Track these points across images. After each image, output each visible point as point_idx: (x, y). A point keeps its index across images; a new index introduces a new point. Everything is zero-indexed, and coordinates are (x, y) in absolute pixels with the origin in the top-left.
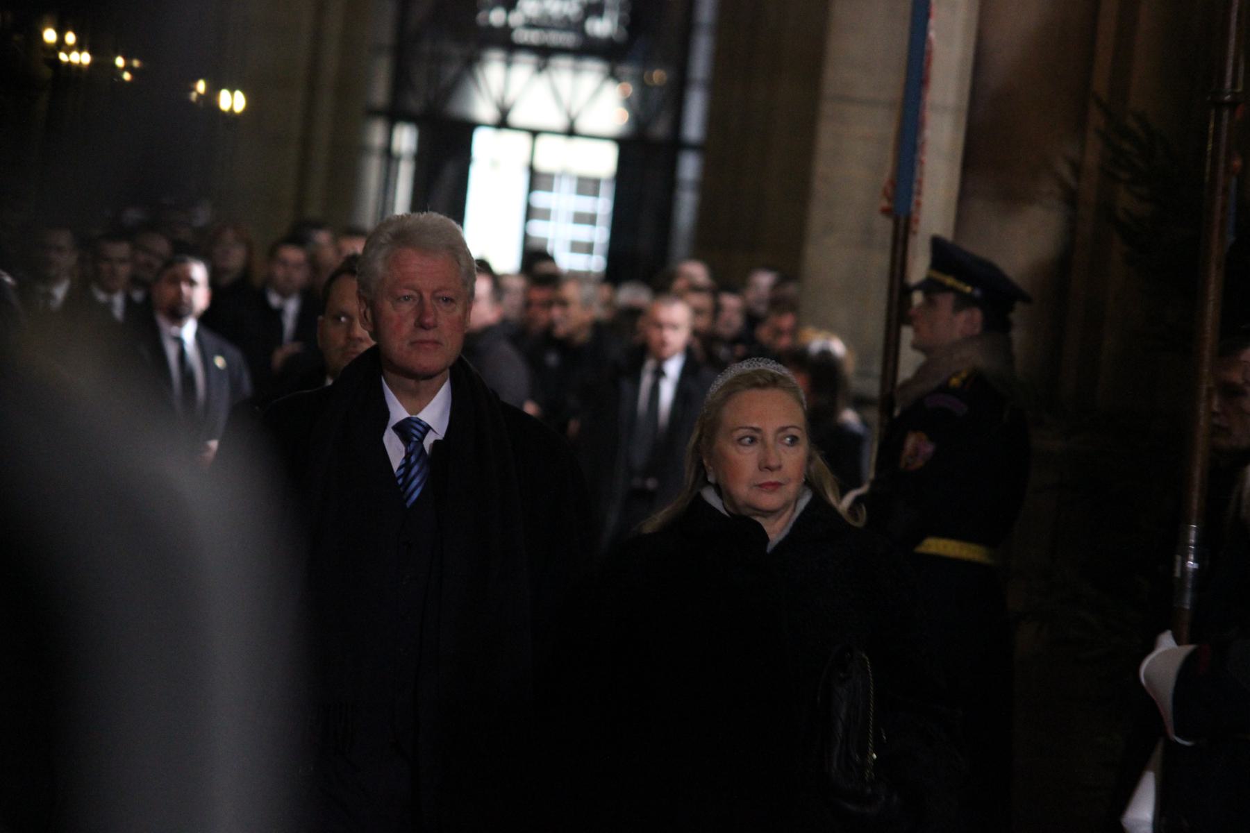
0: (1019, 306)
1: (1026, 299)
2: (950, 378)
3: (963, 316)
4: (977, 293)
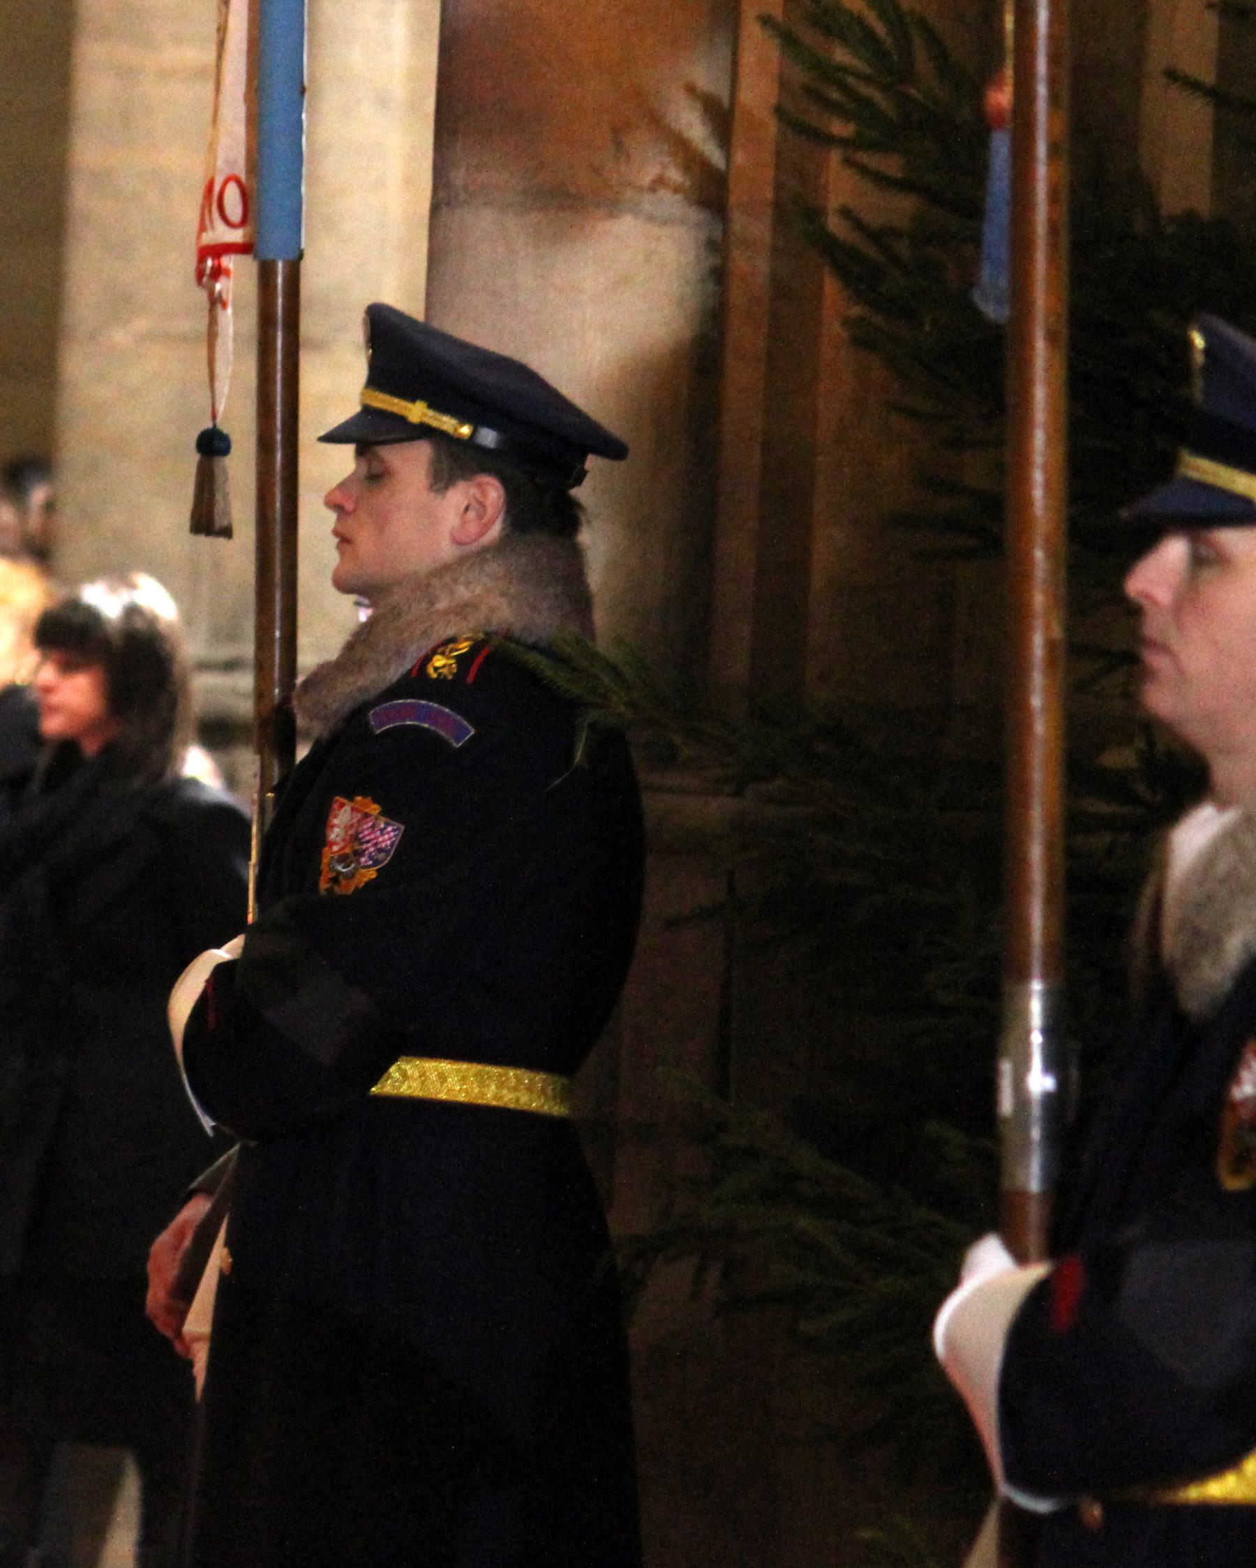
0: (593, 463)
1: (613, 449)
2: (427, 659)
3: (458, 496)
4: (488, 437)
